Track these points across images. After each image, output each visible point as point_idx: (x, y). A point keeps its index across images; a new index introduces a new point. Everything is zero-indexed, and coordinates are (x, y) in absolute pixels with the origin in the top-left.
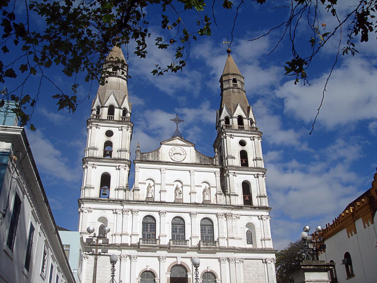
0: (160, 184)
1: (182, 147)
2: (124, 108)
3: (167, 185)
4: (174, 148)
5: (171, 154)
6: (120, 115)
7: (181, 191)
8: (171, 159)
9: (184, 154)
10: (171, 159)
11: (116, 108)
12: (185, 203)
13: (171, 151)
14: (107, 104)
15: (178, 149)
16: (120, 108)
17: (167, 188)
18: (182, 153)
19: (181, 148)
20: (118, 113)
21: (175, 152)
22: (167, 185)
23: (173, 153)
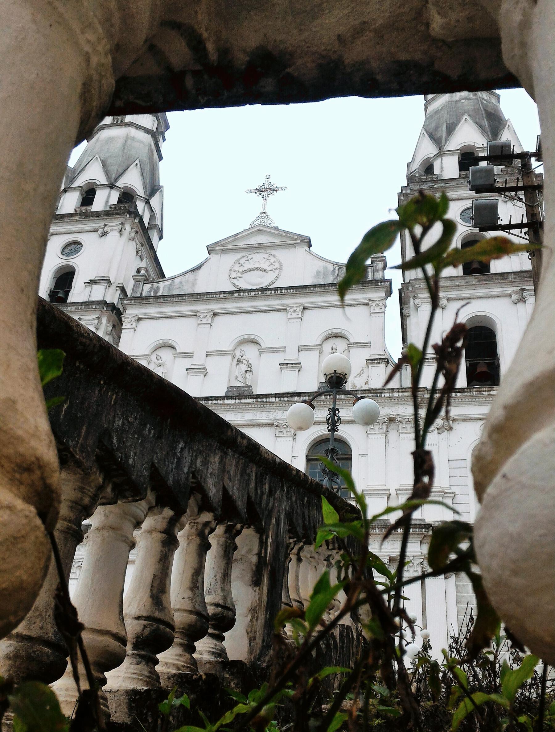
0: (189, 355)
1: (273, 252)
2: (123, 188)
3: (209, 354)
4: (245, 258)
5: (234, 275)
6: (107, 202)
7: (249, 365)
8: (234, 285)
9: (275, 267)
10: (234, 285)
11: (102, 186)
12: (258, 396)
13: (237, 265)
14: (80, 182)
15: (258, 259)
16: (111, 186)
17: (211, 364)
18: (268, 269)
19: (266, 256)
20: (103, 200)
21: (247, 266)
22: (209, 354)
23: (241, 269)
